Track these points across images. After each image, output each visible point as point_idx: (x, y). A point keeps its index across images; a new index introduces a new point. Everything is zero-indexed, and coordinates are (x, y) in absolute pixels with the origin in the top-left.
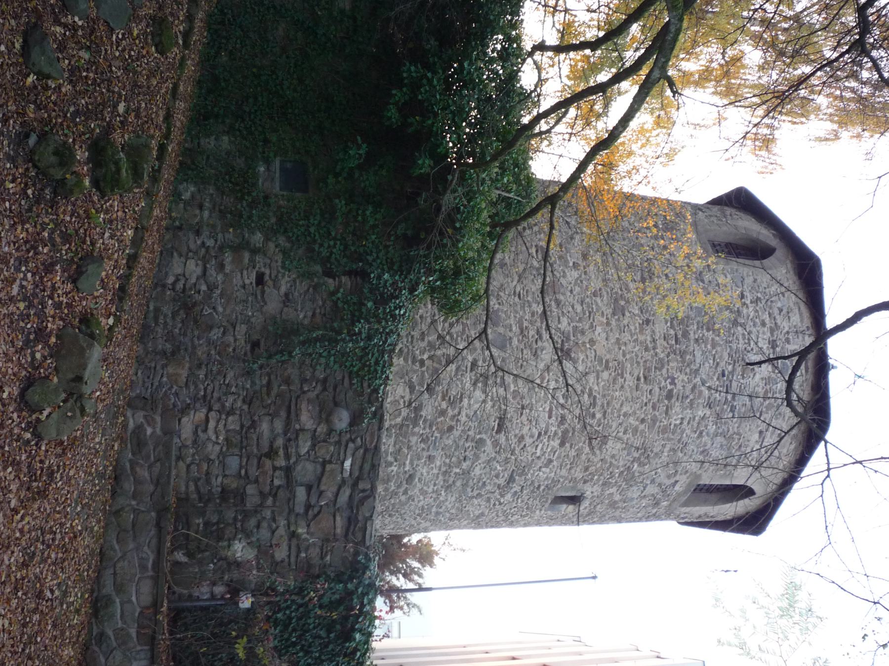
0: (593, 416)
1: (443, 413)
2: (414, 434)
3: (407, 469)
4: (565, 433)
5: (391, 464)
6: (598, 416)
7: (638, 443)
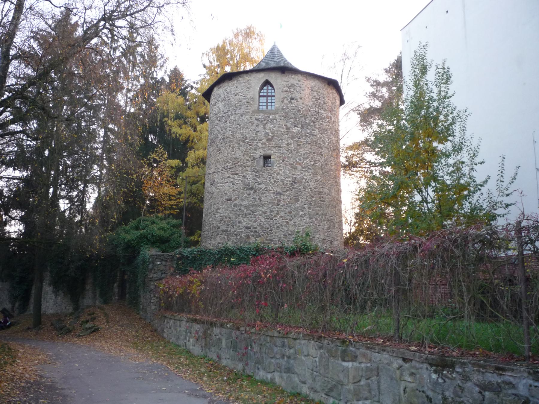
0: (227, 166)
1: (225, 222)
2: (230, 231)
4: (233, 174)
5: (241, 237)
6: (227, 164)
7: (237, 144)
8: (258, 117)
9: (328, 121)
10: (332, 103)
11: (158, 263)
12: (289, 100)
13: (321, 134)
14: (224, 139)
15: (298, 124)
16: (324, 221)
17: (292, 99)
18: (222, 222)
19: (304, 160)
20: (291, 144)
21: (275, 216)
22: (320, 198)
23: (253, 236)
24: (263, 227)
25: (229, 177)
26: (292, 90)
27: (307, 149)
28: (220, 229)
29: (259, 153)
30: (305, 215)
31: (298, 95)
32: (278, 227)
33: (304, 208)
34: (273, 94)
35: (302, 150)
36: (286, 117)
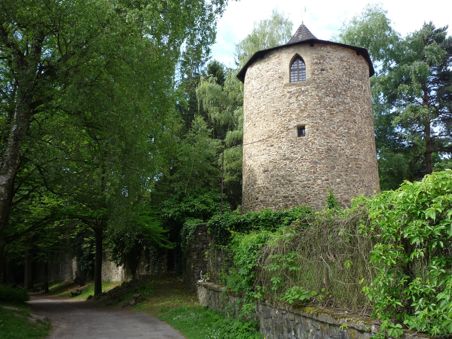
2: (269, 201)
3: (281, 199)
4: (268, 146)
8: (289, 90)
9: (360, 90)
10: (363, 72)
11: (200, 234)
12: (320, 72)
13: (354, 102)
14: (258, 114)
15: (330, 94)
16: (361, 187)
17: (322, 70)
18: (260, 193)
19: (338, 128)
20: (324, 114)
21: (313, 184)
22: (356, 164)
23: (291, 204)
24: (301, 196)
25: (265, 149)
26: (322, 61)
27: (340, 117)
28: (259, 200)
29: (294, 124)
30: (343, 182)
31: (328, 66)
32: (316, 195)
33: (341, 175)
34: (304, 67)
35: (335, 118)
36: (318, 87)
